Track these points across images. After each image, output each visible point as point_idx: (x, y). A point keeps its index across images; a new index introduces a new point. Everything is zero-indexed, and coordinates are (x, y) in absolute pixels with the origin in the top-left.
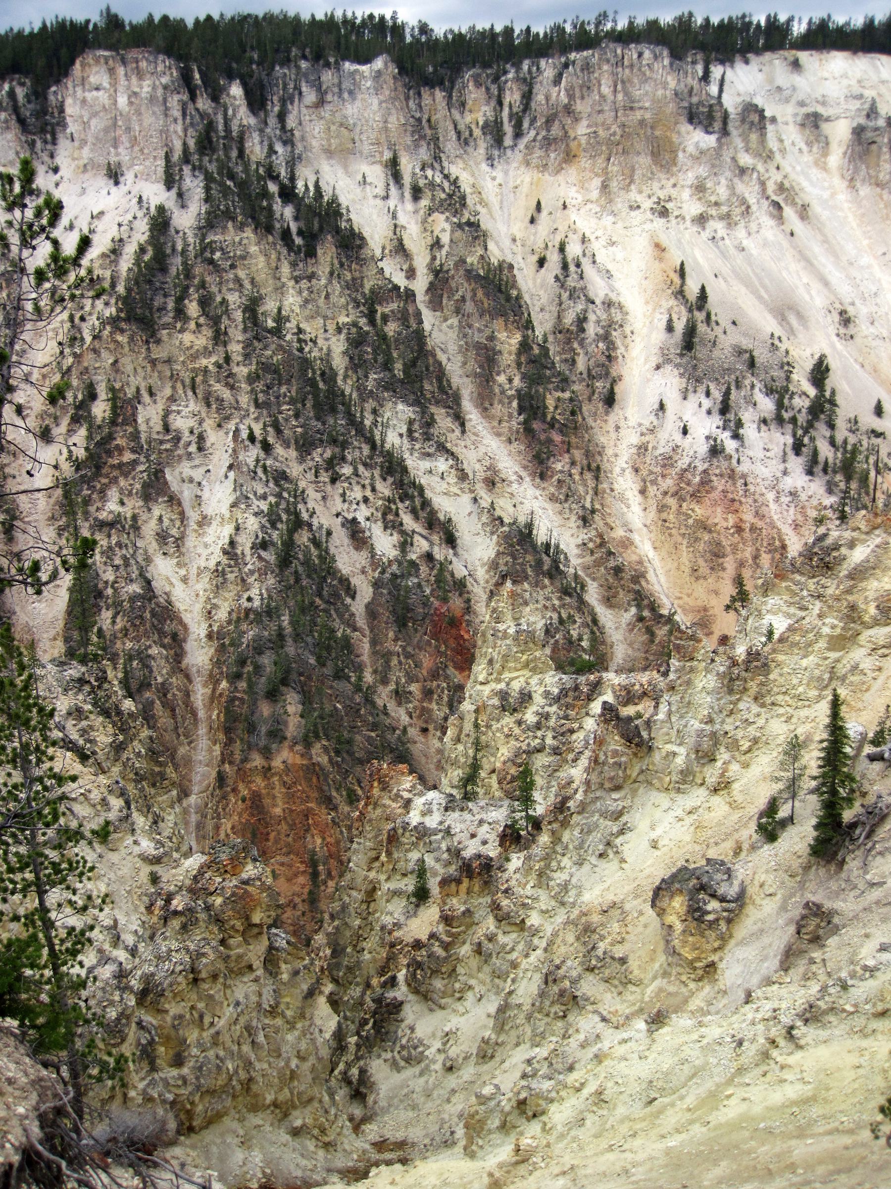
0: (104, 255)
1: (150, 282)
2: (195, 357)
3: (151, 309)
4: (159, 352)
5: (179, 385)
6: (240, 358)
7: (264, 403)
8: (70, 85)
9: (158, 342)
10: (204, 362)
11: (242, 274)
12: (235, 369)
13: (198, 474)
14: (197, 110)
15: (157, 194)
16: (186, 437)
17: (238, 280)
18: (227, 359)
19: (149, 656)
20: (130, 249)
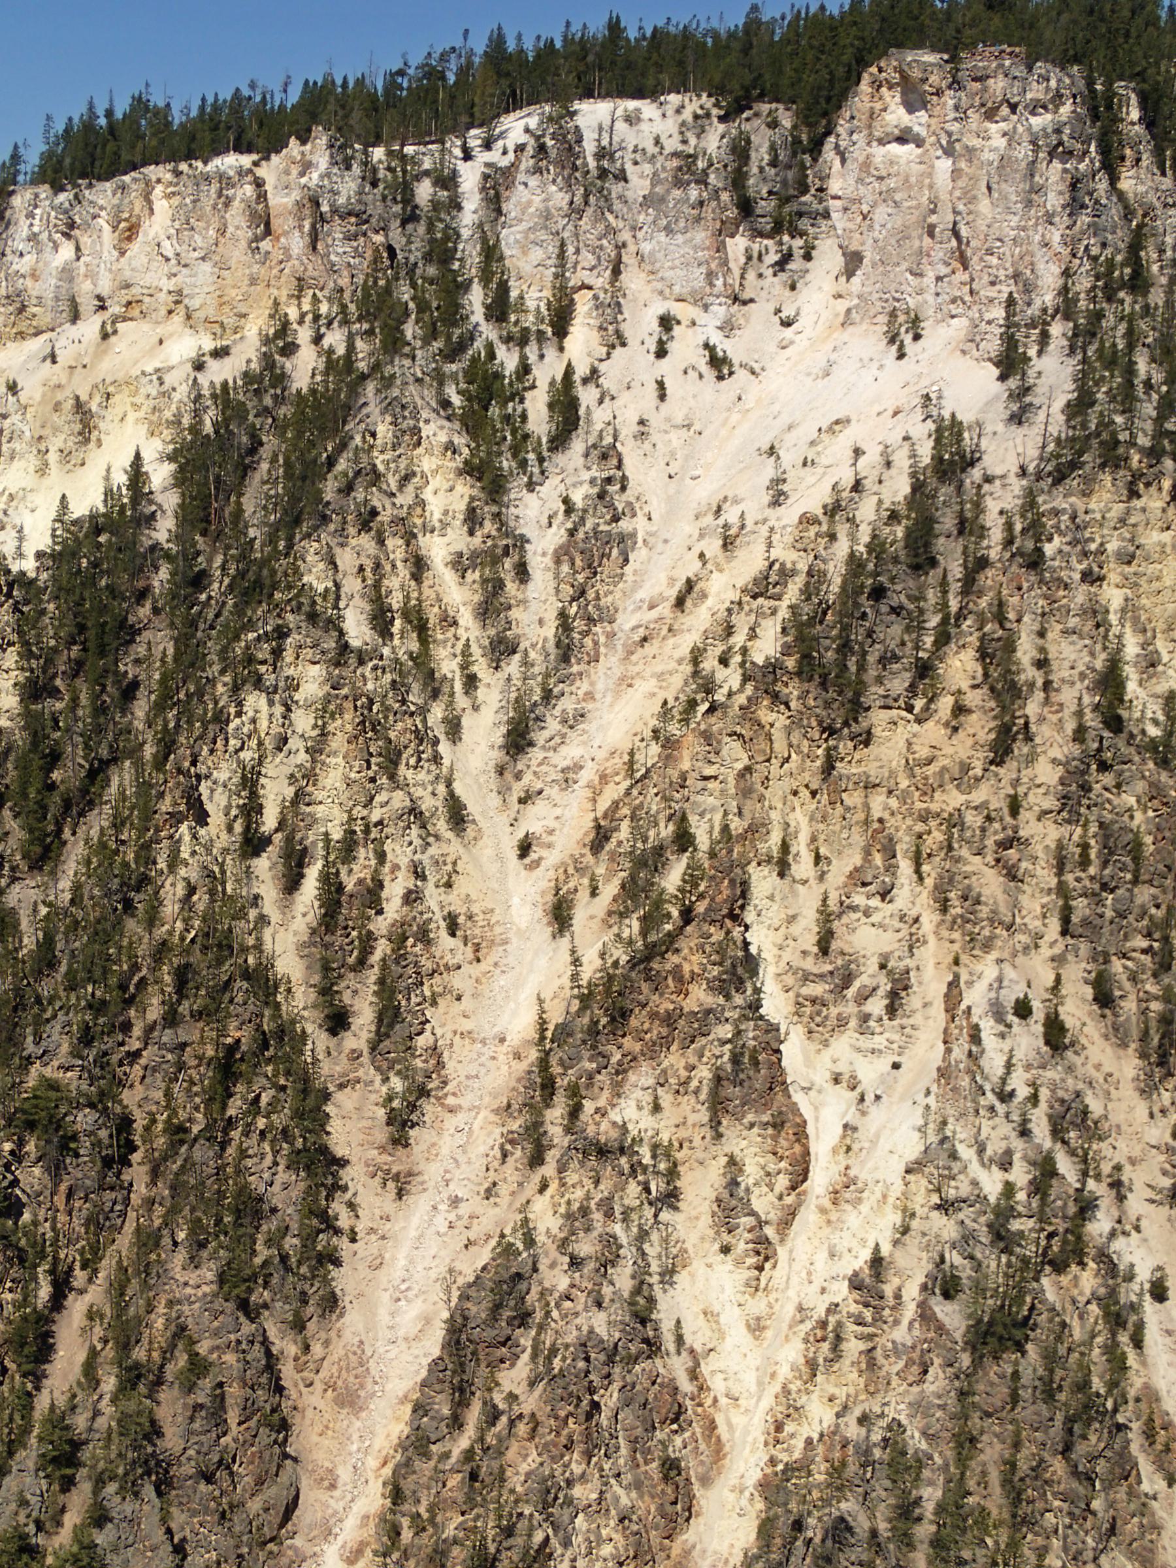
0: (807, 520)
1: (878, 593)
6: (1051, 803)
7: (1086, 922)
8: (842, 127)
9: (866, 739)
11: (1113, 596)
12: (1029, 826)
13: (870, 1072)
14: (1121, 196)
15: (973, 391)
16: (868, 975)
17: (1096, 614)
18: (1015, 807)
19: (569, 1501)
20: (866, 511)
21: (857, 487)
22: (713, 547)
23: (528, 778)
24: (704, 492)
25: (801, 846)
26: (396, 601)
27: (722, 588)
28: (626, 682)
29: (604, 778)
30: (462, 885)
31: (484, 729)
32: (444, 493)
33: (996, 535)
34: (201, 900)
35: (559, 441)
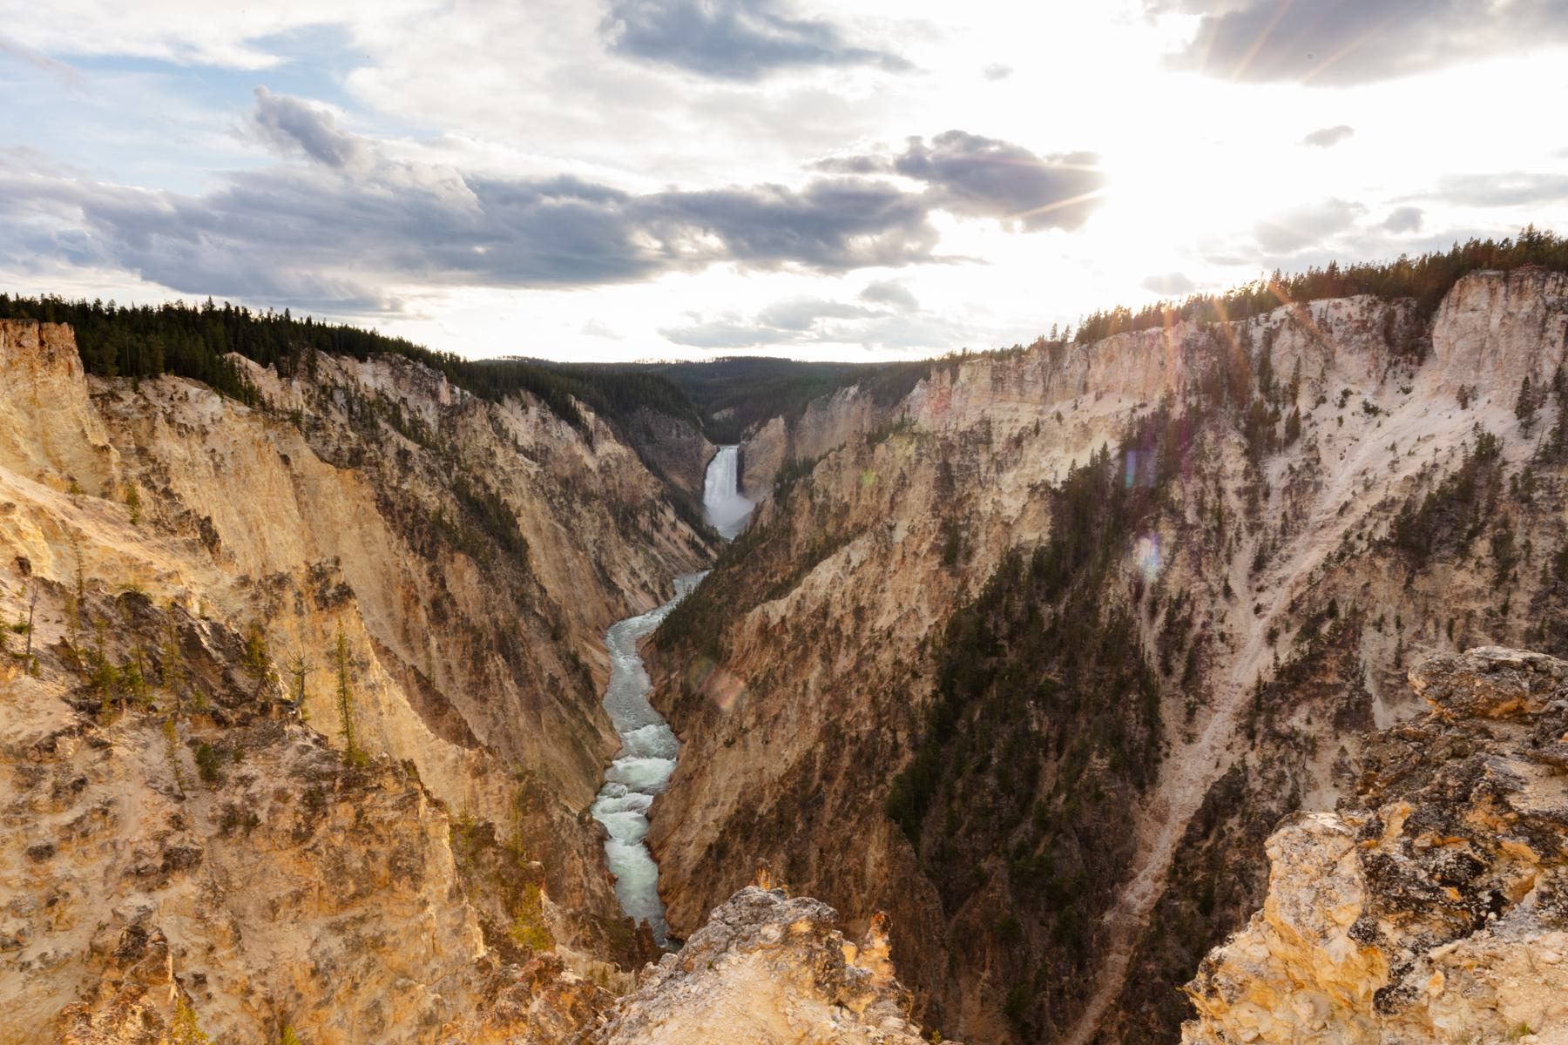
0: (1407, 478)
2: (1465, 597)
3: (1430, 540)
4: (1421, 584)
5: (1430, 624)
10: (1473, 605)
20: (1439, 477)
21: (1435, 466)
22: (1359, 489)
23: (1262, 582)
24: (1353, 467)
25: (1390, 619)
26: (1209, 506)
27: (1362, 507)
28: (1312, 545)
29: (1298, 584)
30: (1228, 622)
31: (1244, 559)
32: (1233, 462)
33: (1507, 488)
34: (1116, 618)
35: (1288, 442)
